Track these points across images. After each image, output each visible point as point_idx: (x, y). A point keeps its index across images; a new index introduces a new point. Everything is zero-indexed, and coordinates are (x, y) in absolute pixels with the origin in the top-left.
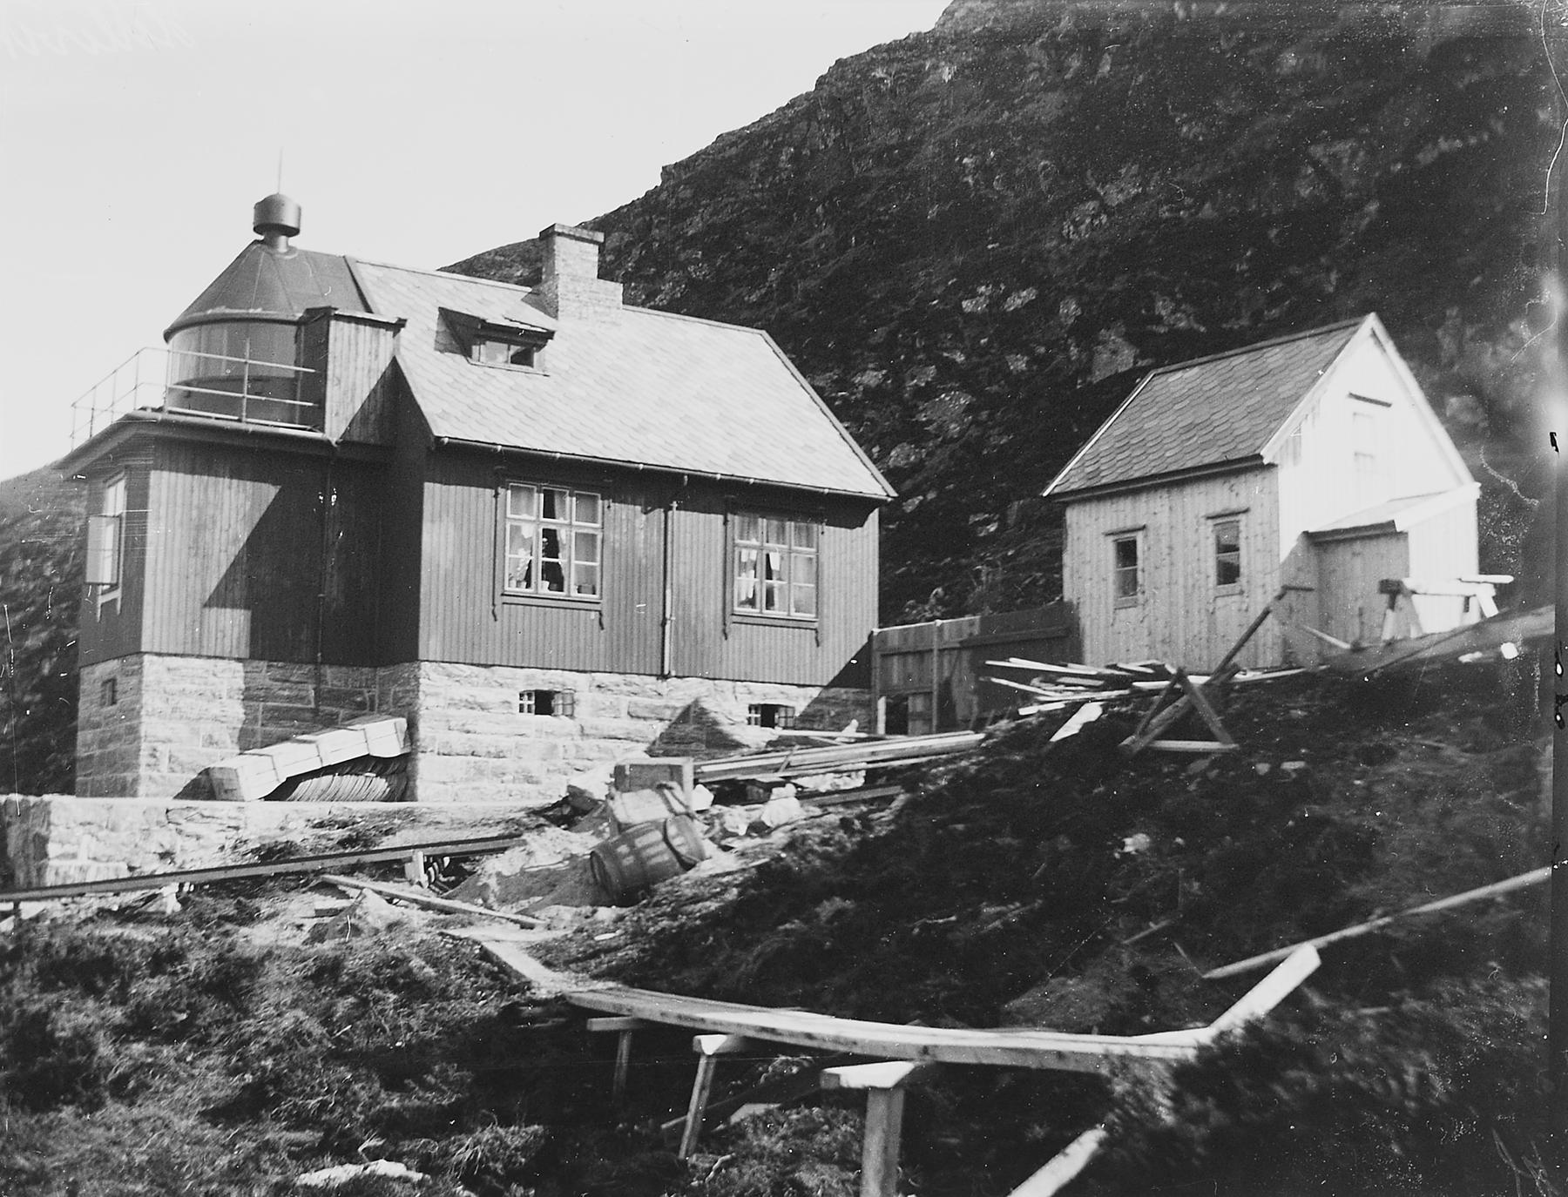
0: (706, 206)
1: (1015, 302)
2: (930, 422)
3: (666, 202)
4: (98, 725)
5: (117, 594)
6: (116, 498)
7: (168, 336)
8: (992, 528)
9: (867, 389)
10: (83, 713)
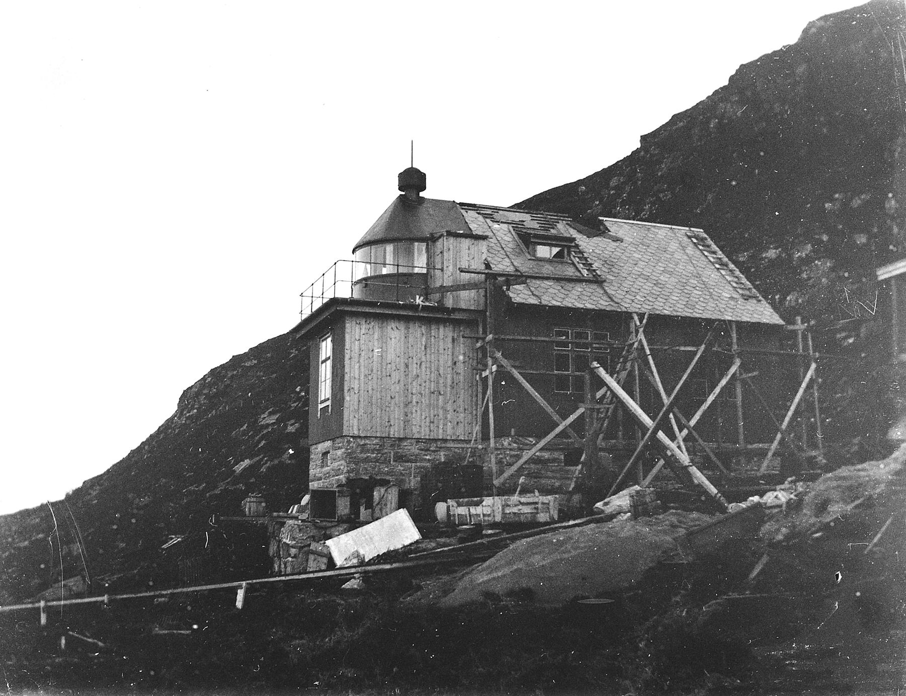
0: (667, 158)
1: (856, 203)
2: (809, 278)
3: (643, 157)
4: (320, 479)
5: (329, 403)
6: (326, 348)
7: (354, 251)
8: (851, 341)
9: (770, 260)
10: (312, 472)
